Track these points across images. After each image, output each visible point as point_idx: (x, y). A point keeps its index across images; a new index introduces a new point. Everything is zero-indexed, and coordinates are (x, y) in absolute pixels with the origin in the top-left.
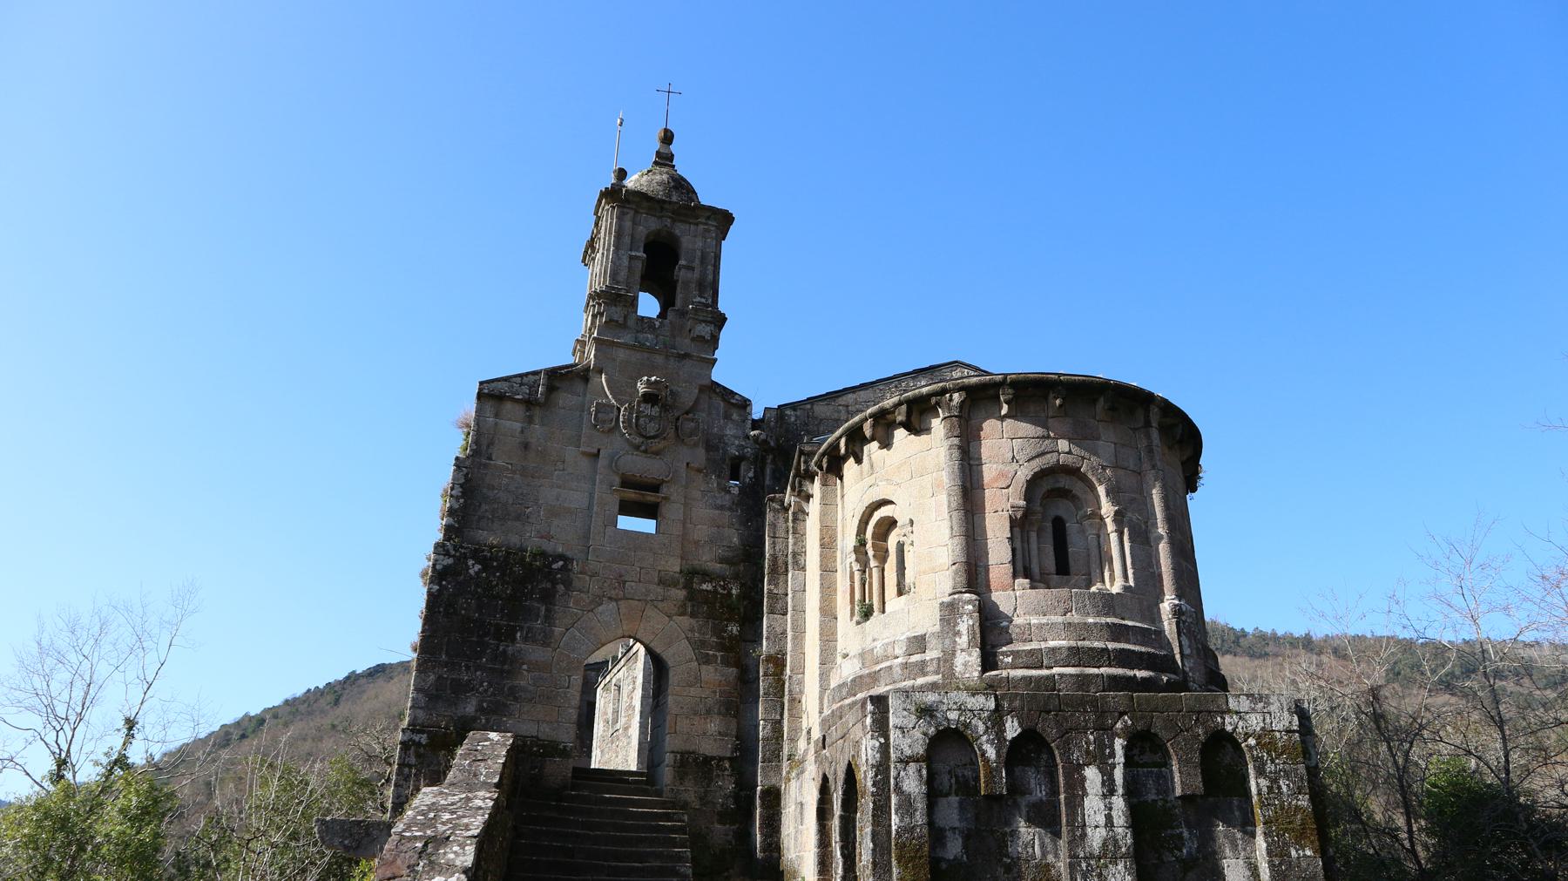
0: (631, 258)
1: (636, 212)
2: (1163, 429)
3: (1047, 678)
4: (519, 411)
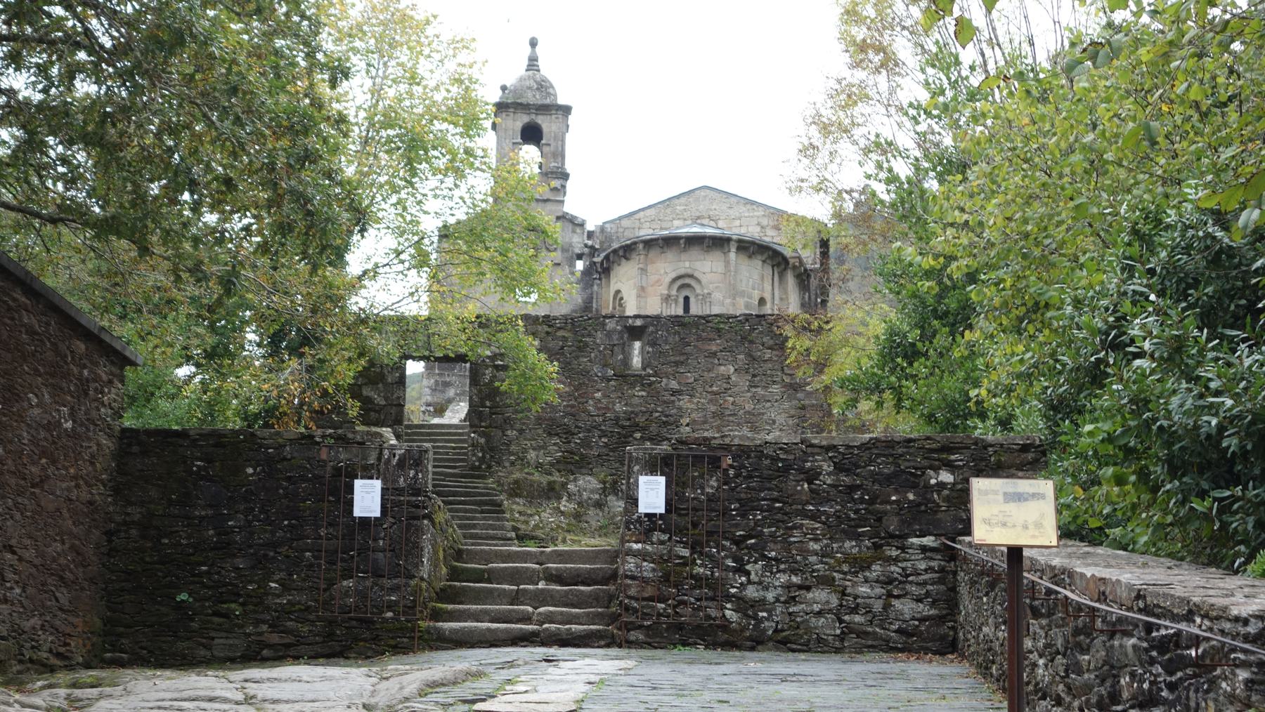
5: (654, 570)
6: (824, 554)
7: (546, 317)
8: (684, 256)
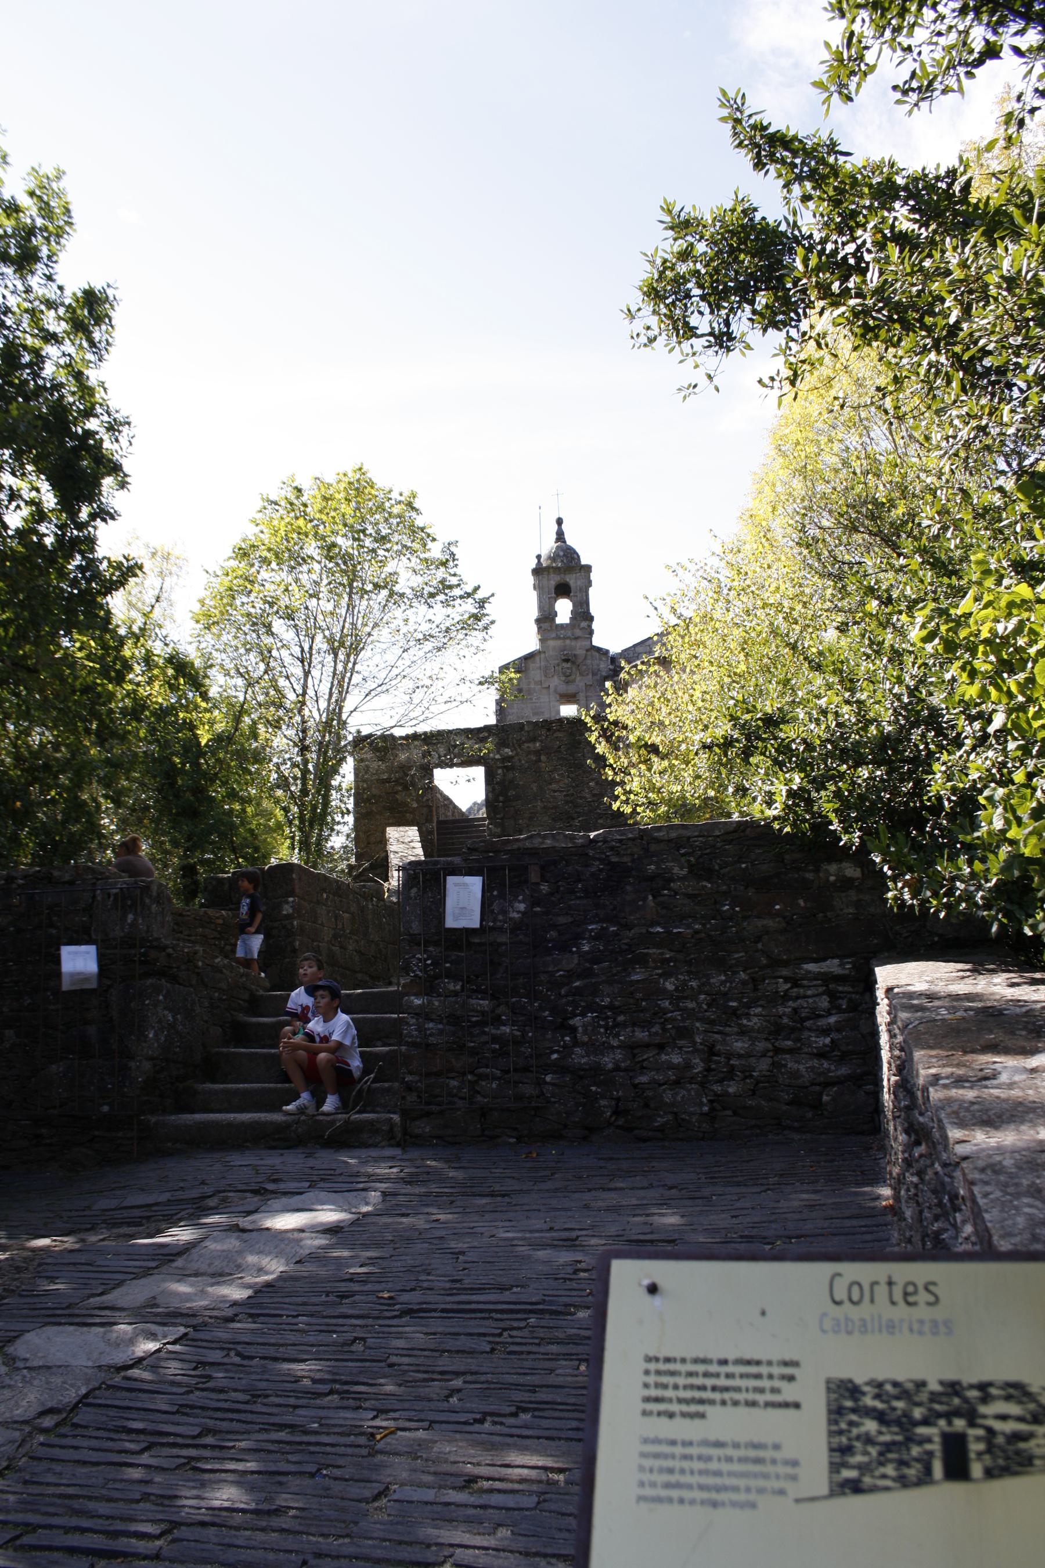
5: (441, 1032)
6: (681, 994)
7: (545, 721)
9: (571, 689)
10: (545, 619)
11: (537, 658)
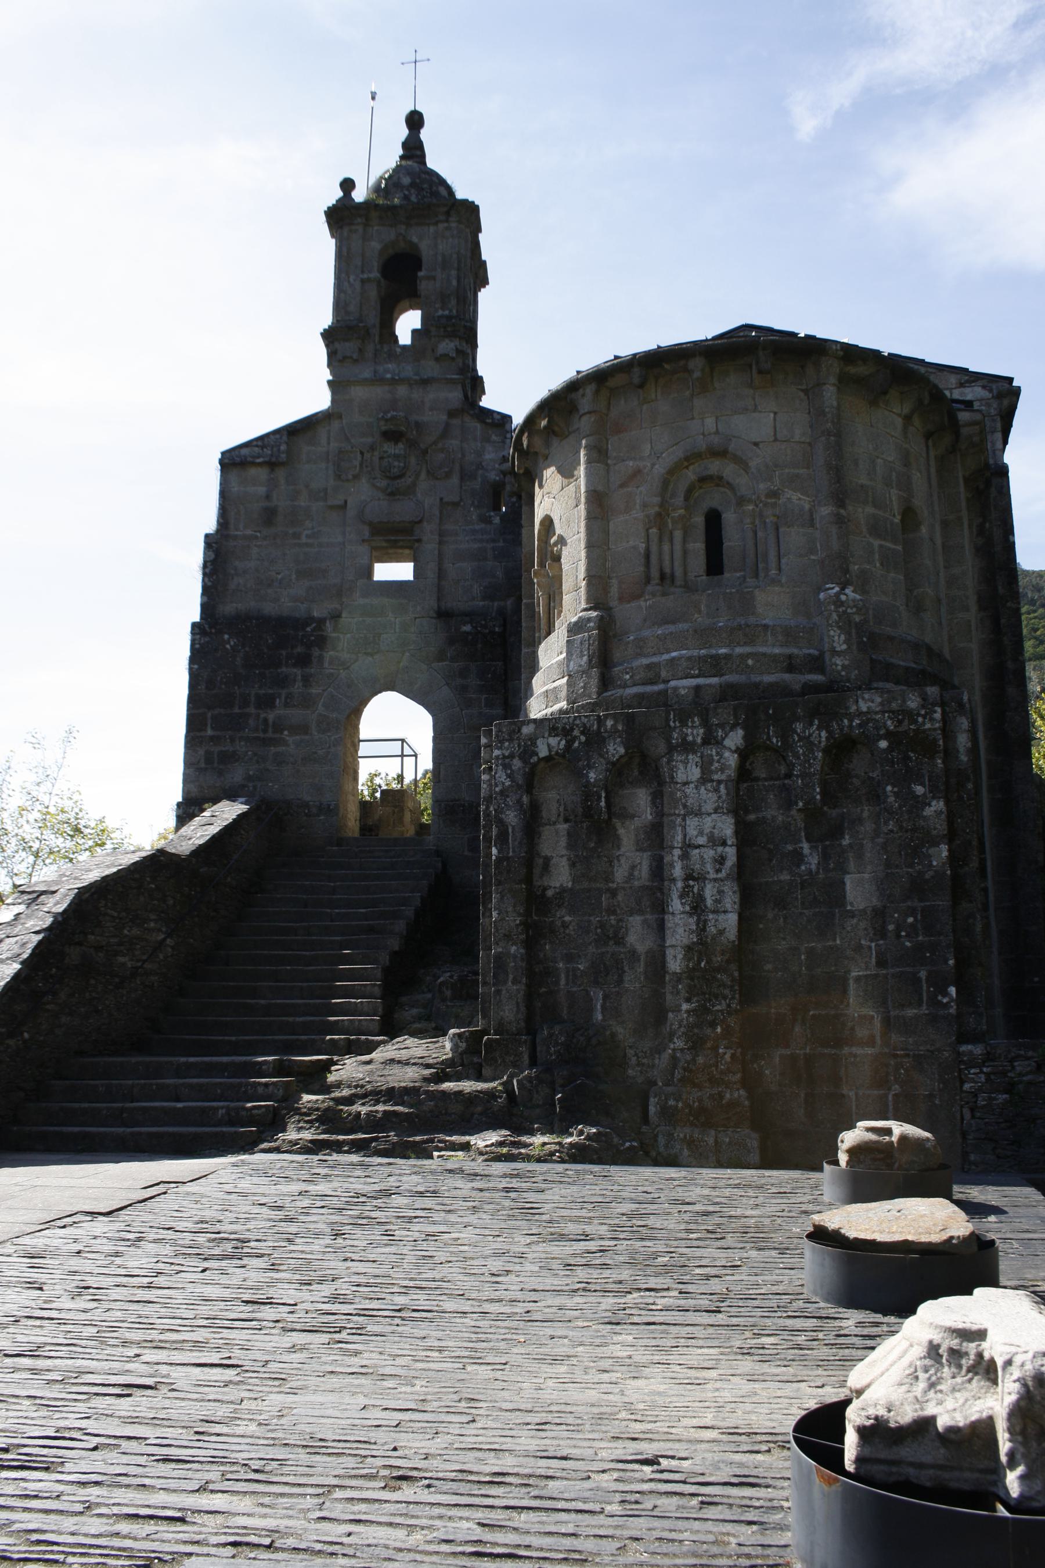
0: (363, 281)
1: (366, 225)
2: (844, 381)
3: (659, 693)
4: (262, 473)
8: (698, 403)
9: (403, 510)
10: (352, 339)
11: (322, 433)
